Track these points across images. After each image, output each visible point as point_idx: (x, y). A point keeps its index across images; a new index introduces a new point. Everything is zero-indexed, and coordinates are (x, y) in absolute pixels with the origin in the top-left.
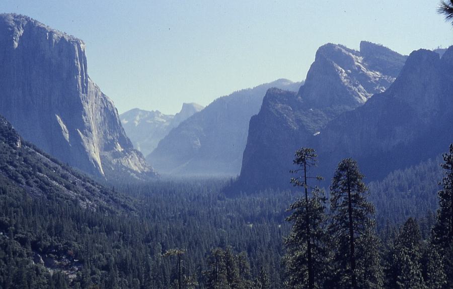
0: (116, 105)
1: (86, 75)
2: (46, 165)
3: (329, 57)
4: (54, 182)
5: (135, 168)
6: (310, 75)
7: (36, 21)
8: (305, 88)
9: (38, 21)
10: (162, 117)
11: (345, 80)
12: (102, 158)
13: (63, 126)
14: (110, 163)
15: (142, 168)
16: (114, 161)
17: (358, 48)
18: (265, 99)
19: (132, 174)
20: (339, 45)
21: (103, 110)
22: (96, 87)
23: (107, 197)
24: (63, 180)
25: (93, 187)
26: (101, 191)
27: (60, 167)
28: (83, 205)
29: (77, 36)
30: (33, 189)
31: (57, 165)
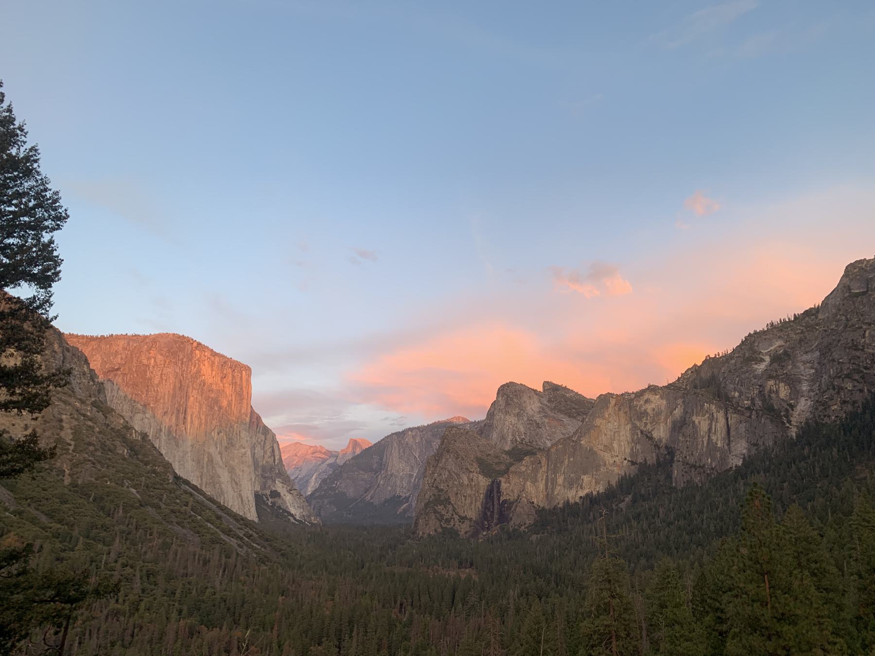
0: (278, 438)
2: (201, 503)
4: (209, 525)
5: (293, 511)
6: (491, 415)
7: (199, 344)
8: (484, 428)
10: (325, 453)
12: (258, 497)
13: (217, 458)
17: (540, 389)
18: (443, 438)
22: (259, 418)
23: (266, 544)
24: (218, 522)
25: (251, 532)
26: (260, 537)
29: (244, 361)
30: (184, 531)
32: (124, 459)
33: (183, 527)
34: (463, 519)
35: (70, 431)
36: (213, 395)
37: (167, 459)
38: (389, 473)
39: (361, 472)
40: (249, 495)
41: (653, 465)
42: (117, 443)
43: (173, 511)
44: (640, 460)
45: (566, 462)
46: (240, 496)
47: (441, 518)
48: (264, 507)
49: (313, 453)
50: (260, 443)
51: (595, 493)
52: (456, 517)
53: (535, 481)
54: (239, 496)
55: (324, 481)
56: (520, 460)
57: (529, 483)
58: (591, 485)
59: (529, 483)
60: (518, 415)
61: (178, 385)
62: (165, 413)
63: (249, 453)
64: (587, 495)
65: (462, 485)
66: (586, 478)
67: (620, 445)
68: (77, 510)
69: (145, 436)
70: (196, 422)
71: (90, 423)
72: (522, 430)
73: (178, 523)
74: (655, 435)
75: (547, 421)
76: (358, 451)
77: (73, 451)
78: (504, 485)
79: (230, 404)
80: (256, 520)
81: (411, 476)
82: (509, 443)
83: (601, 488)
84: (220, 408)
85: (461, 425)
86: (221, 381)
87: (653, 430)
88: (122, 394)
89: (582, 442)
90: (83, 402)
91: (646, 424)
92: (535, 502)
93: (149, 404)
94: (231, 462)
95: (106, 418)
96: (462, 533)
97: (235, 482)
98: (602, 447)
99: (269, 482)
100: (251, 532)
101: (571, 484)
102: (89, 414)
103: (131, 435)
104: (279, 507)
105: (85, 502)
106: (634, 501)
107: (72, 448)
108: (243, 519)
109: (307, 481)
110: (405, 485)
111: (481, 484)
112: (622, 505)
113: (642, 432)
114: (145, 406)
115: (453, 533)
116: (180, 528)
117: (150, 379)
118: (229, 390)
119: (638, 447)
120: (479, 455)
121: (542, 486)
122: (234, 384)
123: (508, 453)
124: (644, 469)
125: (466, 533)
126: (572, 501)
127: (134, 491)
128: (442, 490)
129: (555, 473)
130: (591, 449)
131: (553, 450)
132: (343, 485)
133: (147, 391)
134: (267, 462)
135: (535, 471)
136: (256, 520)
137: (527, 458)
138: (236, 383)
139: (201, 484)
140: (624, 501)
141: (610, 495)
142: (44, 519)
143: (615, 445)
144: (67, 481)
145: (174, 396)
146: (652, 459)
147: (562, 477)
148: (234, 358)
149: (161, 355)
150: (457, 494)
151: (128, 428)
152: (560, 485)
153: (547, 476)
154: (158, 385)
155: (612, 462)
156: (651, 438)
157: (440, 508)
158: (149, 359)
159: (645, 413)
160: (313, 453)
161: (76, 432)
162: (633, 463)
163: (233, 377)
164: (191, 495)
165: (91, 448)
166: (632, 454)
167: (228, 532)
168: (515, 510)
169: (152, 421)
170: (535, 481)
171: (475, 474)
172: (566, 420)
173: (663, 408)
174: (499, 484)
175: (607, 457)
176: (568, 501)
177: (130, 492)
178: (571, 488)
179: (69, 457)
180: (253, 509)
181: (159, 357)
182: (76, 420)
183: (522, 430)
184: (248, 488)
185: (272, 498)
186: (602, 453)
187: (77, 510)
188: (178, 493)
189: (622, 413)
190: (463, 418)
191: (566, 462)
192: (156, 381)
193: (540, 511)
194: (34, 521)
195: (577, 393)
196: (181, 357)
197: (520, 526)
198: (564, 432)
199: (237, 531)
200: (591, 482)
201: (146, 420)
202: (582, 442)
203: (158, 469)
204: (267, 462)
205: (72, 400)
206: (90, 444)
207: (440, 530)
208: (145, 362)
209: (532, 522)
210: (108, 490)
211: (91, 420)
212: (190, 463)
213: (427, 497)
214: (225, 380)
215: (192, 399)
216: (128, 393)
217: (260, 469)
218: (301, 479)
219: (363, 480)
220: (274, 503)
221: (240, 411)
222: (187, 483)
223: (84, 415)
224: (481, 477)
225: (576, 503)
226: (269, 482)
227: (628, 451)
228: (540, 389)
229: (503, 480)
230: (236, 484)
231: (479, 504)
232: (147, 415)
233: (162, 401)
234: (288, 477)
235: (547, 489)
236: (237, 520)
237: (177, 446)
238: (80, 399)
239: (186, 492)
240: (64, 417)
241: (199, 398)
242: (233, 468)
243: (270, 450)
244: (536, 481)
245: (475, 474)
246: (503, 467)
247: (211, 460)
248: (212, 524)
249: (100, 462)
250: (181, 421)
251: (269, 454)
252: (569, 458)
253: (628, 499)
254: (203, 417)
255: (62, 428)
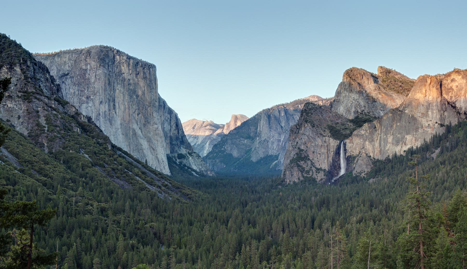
0: (180, 116)
1: (156, 92)
3: (353, 78)
5: (195, 167)
6: (338, 93)
9: (121, 50)
11: (367, 98)
12: (169, 159)
13: (139, 132)
14: (176, 163)
15: (201, 167)
16: (178, 160)
19: (193, 172)
20: (361, 69)
21: (169, 120)
22: (164, 102)
24: (143, 176)
25: (166, 183)
27: (140, 166)
28: (162, 196)
30: (122, 183)
31: (138, 164)
32: (79, 135)
33: (120, 180)
34: (318, 170)
35: (44, 118)
36: (131, 88)
37: (105, 134)
38: (263, 139)
39: (242, 139)
40: (163, 157)
41: (456, 125)
42: (73, 125)
43: (113, 169)
44: (447, 123)
45: (394, 126)
46: (157, 157)
47: (302, 170)
48: (174, 165)
49: (206, 126)
50: (167, 121)
51: (415, 148)
52: (314, 169)
53: (372, 141)
54: (157, 158)
55: (215, 146)
56: (361, 126)
57: (367, 143)
58: (412, 142)
59: (367, 143)
60: (360, 93)
61: (107, 82)
62: (101, 102)
63: (160, 127)
64: (409, 149)
65: (317, 146)
66: (409, 137)
67: (432, 113)
68: (54, 169)
69: (89, 119)
70: (122, 107)
71: (54, 112)
72: (362, 103)
73: (118, 177)
74: (458, 105)
75: (380, 96)
76: (239, 124)
77: (47, 131)
78: (349, 145)
79: (144, 94)
80: (169, 174)
81: (279, 141)
82: (352, 114)
83: (419, 144)
84: (137, 96)
85: (316, 101)
86: (136, 77)
87: (456, 102)
88: (72, 91)
89: (406, 112)
90: (49, 98)
91: (451, 97)
92: (372, 155)
93: (90, 97)
94: (148, 134)
95: (64, 108)
96: (318, 180)
97: (153, 149)
98: (419, 115)
99: (177, 148)
100: (166, 183)
101: (397, 142)
102: (53, 106)
103: (80, 119)
104: (185, 165)
105: (58, 164)
106: (442, 152)
107: (46, 129)
108: (160, 174)
109: (203, 146)
110: (275, 147)
111: (332, 144)
112: (434, 155)
113: (448, 103)
114: (88, 98)
115: (313, 181)
116: (119, 180)
117: (89, 79)
118: (142, 83)
119: (446, 114)
120: (330, 123)
121: (377, 144)
122: (145, 78)
123: (351, 121)
124: (449, 129)
125: (322, 179)
126: (398, 154)
127: (87, 156)
128: (303, 150)
129: (386, 134)
130: (413, 116)
131: (385, 118)
132: (229, 149)
133: (88, 88)
134: (173, 134)
135: (372, 134)
136: (169, 174)
137: (366, 125)
138: (146, 77)
139: (130, 151)
140: (435, 152)
141: (426, 148)
142: (38, 176)
143: (430, 113)
144: (47, 151)
145: (105, 90)
146: (454, 122)
147: (392, 137)
148: (144, 60)
149: (94, 61)
150: (314, 152)
151: (78, 114)
152: (390, 143)
153: (380, 137)
154: (94, 83)
155: (427, 125)
156: (454, 107)
157: (302, 163)
158: (86, 65)
159: (451, 88)
160: (206, 126)
161: (48, 120)
162: (442, 125)
163: (144, 73)
164: (123, 157)
165: (58, 129)
166: (442, 118)
167: (151, 184)
168: (357, 161)
169: (93, 108)
170: (372, 141)
171: (327, 138)
172: (395, 95)
173: (463, 85)
174: (345, 145)
175: (424, 122)
176: (396, 154)
177: (84, 157)
178: (398, 145)
179: (45, 135)
180: (167, 167)
181: (93, 63)
182: (46, 110)
183: (362, 103)
184: (162, 152)
185: (179, 159)
186: (420, 119)
187: (54, 169)
188: (115, 156)
189: (434, 89)
190: (318, 97)
191: (395, 125)
192: (93, 80)
193: (376, 162)
194: (31, 176)
195: (403, 76)
196: (107, 61)
197: (360, 173)
198: (394, 104)
199: (157, 183)
200: (412, 139)
201: (89, 108)
202: (406, 112)
203: (101, 141)
204: (173, 134)
205: (43, 98)
206: (56, 126)
207: (302, 179)
208: (84, 67)
209: (369, 170)
210: (71, 156)
211: (55, 110)
212: (121, 136)
213: (292, 155)
214: (138, 76)
215: (117, 91)
216: (76, 90)
217: (169, 139)
218: (199, 145)
219: (243, 144)
220: (181, 163)
221: (151, 98)
222: (120, 149)
223: (51, 107)
224: (331, 140)
225: (401, 155)
226: (177, 148)
227: (438, 117)
228: (376, 72)
229: (347, 141)
230: (154, 150)
231: (331, 159)
232: (90, 105)
233: (98, 94)
234: (189, 144)
235: (380, 146)
236: (156, 175)
237: (111, 124)
238: (47, 97)
239: (120, 156)
240: (39, 109)
241: (122, 90)
242: (150, 139)
243: (175, 125)
244: (373, 141)
245: (327, 138)
246: (348, 132)
247: (135, 134)
248: (140, 177)
249: (64, 138)
250: (112, 108)
251: (174, 128)
252: (396, 123)
253: (438, 151)
254: (126, 104)
255: (39, 117)
